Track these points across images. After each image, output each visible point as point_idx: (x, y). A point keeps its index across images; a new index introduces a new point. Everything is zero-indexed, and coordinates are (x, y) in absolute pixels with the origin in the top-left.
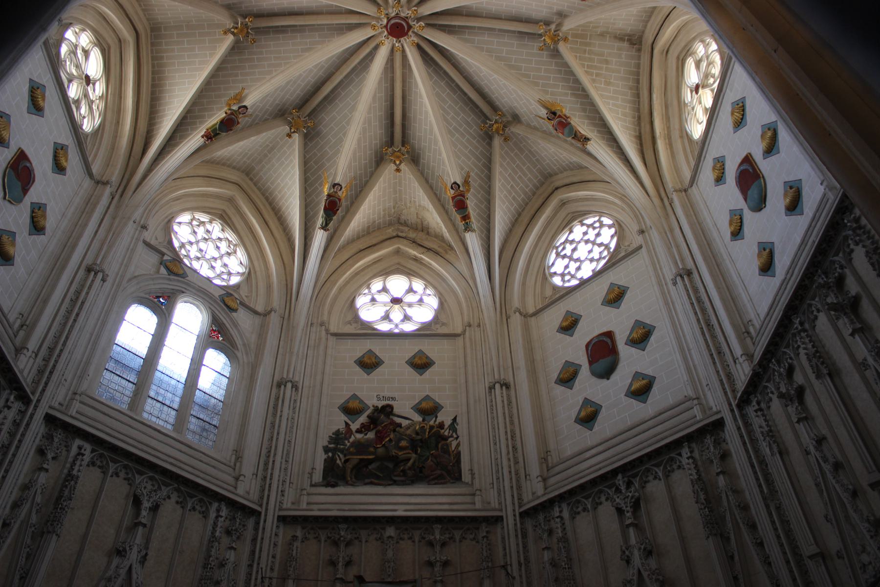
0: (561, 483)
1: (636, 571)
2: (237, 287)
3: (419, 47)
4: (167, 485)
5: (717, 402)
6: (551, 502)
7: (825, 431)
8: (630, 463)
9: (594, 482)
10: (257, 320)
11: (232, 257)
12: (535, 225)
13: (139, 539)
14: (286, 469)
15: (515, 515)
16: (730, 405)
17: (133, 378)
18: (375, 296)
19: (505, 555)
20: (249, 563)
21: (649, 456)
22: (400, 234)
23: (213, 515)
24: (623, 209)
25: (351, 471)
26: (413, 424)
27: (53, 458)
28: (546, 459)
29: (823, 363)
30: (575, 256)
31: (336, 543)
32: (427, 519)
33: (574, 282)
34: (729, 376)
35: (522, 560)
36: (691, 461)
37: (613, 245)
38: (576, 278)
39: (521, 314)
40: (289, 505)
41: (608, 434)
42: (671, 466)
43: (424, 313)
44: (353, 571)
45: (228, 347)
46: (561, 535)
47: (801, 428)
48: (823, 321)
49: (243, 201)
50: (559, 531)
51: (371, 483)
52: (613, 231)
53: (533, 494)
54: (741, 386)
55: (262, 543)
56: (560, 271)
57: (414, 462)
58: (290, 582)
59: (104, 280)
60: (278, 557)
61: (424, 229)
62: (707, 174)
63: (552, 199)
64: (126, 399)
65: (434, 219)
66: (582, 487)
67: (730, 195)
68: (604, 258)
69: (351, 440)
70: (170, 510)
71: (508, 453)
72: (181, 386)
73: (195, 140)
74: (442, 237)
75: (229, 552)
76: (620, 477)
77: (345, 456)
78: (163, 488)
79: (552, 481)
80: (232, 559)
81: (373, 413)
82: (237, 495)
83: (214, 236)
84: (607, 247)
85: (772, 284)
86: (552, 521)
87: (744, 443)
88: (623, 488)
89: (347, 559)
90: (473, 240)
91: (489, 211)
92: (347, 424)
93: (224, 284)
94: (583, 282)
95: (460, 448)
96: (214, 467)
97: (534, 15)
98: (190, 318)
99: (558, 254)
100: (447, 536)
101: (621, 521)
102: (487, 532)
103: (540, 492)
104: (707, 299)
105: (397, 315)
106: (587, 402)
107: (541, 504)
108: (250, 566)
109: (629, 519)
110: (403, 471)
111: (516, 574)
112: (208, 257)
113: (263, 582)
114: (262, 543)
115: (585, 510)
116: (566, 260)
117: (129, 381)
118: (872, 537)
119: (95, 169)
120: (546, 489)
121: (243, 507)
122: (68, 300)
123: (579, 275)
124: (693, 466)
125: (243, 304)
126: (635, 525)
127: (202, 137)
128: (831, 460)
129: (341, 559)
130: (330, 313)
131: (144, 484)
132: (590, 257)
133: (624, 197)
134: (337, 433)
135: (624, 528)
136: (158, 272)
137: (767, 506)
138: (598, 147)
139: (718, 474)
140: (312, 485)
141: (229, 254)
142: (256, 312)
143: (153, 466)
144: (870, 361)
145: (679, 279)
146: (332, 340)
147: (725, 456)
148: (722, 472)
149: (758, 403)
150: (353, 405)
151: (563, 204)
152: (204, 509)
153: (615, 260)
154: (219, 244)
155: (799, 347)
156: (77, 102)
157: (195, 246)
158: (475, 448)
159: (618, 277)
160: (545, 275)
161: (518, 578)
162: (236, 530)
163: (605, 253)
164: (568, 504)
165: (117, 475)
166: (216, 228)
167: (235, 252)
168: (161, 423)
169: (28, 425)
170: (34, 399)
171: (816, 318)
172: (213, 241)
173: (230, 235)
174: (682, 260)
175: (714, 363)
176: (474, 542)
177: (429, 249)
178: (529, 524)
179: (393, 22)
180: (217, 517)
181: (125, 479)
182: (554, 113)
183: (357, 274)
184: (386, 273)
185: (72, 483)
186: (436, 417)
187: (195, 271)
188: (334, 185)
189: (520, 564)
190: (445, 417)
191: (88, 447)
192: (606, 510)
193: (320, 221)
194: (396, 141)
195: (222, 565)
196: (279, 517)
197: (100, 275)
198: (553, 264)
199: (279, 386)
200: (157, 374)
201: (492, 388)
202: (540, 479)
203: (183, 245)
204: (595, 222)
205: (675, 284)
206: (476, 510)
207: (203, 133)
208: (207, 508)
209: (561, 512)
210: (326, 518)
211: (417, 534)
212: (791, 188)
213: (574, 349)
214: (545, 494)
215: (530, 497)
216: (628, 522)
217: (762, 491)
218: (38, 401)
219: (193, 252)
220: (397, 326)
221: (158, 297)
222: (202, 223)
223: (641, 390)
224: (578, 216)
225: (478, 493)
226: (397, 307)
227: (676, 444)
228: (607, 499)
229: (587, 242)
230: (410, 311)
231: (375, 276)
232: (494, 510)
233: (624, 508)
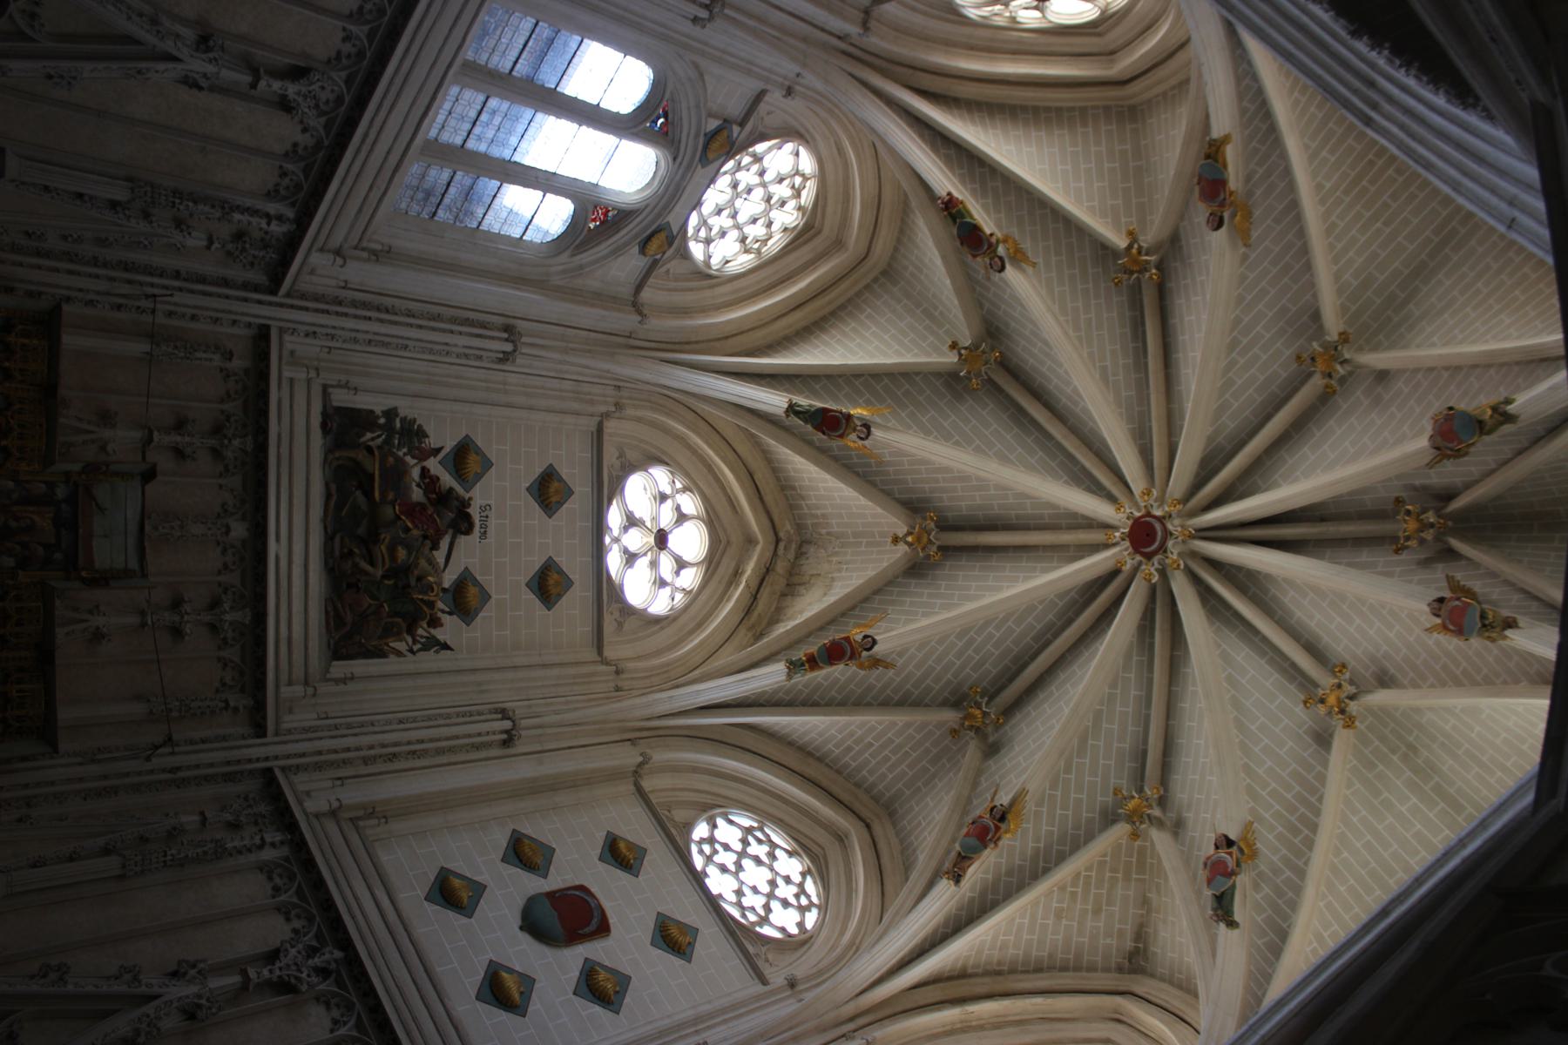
1: (156, 990)
2: (685, 255)
3: (1114, 573)
4: (327, 127)
6: (291, 826)
8: (365, 973)
9: (328, 905)
10: (626, 291)
11: (737, 246)
12: (800, 789)
13: (229, 75)
14: (355, 341)
15: (267, 759)
17: (522, 69)
18: (669, 502)
19: (192, 742)
21: (376, 1009)
22: (782, 545)
23: (272, 208)
24: (833, 948)
26: (439, 572)
28: (371, 815)
30: (746, 863)
31: (217, 430)
32: (261, 597)
33: (698, 862)
35: (181, 774)
37: (767, 931)
38: (706, 865)
39: (640, 765)
40: (289, 346)
41: (420, 931)
43: (638, 588)
45: (576, 237)
46: (229, 845)
49: (837, 264)
50: (236, 843)
51: (328, 496)
52: (794, 930)
53: (308, 793)
56: (718, 834)
57: (366, 573)
59: (695, 20)
60: (193, 325)
61: (793, 586)
63: (846, 818)
64: (485, 57)
65: (810, 606)
66: (319, 884)
68: (744, 916)
69: (408, 459)
70: (282, 132)
71: (383, 746)
72: (506, 154)
73: (943, 181)
74: (778, 621)
76: (338, 954)
77: (379, 447)
78: (323, 120)
79: (331, 827)
80: (190, 242)
81: (458, 498)
82: (310, 250)
83: (774, 214)
84: (764, 920)
88: (317, 961)
90: (772, 676)
91: (827, 705)
92: (439, 450)
93: (690, 231)
94: (698, 878)
95: (392, 658)
96: (360, 210)
97: (1177, 778)
98: (629, 170)
99: (749, 830)
100: (230, 634)
102: (236, 710)
103: (310, 805)
105: (636, 540)
106: (479, 889)
107: (288, 808)
108: (177, 275)
110: (351, 553)
112: (738, 203)
113: (147, 296)
115: (276, 889)
116: (738, 847)
117: (516, 63)
120: (317, 816)
121: (285, 262)
125: (654, 264)
126: (245, 986)
127: (949, 194)
129: (187, 439)
130: (639, 420)
132: (746, 890)
133: (855, 948)
134: (421, 434)
136: (710, 115)
138: (943, 899)
140: (325, 388)
141: (743, 240)
142: (639, 288)
143: (361, 103)
150: (473, 462)
151: (841, 839)
152: (283, 192)
153: (740, 935)
154: (760, 222)
157: (757, 180)
158: (394, 684)
159: (710, 942)
160: (710, 808)
162: (244, 250)
163: (752, 918)
164: (287, 859)
165: (347, 39)
166: (787, 217)
167: (747, 251)
168: (441, 118)
172: (766, 212)
173: (776, 243)
177: (755, 597)
179: (1158, 527)
180: (268, 217)
182: (1002, 818)
183: (710, 468)
184: (712, 521)
186: (450, 613)
187: (713, 181)
188: (867, 426)
190: (450, 628)
192: (275, 930)
193: (803, 401)
194: (948, 536)
195: (179, 224)
196: (268, 327)
197: (704, 14)
198: (731, 822)
199: (507, 329)
200: (529, 113)
201: (504, 714)
202: (335, 805)
203: (758, 159)
204: (808, 897)
206: (277, 686)
207: (956, 194)
209: (273, 845)
210: (264, 413)
213: (576, 864)
214: (306, 814)
215: (301, 788)
216: (252, 973)
219: (747, 178)
220: (616, 540)
221: (666, 116)
222: (797, 193)
223: (501, 991)
224: (819, 867)
225: (310, 691)
226: (652, 540)
228: (295, 931)
229: (773, 883)
230: (643, 563)
231: (706, 500)
232: (277, 723)
233: (278, 964)
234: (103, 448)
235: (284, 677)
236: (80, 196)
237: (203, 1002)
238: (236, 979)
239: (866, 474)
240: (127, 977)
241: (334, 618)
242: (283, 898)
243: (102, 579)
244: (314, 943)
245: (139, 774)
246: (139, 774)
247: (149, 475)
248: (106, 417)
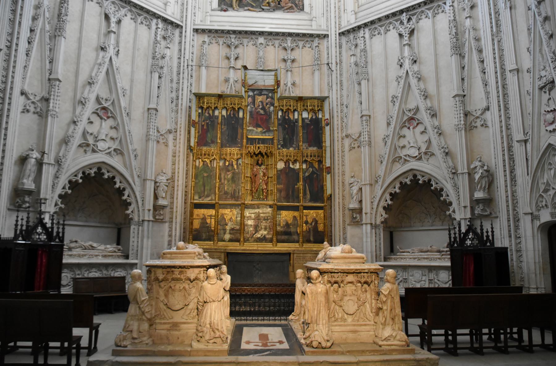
1: (405, 72)
4: (124, 7)
6: (359, 27)
8: (412, 6)
9: (387, 17)
19: (328, 58)
20: (179, 56)
23: (154, 27)
31: (229, 46)
32: (284, 34)
35: (338, 61)
36: (451, 8)
40: (199, 22)
42: (438, 10)
44: (239, 64)
46: (363, 47)
50: (362, 45)
51: (249, 10)
53: (348, 22)
55: (185, 45)
58: (204, 68)
60: (195, 53)
66: (380, 19)
75: (166, 49)
76: (404, 14)
78: (121, 9)
86: (358, 39)
88: (405, 22)
89: (236, 56)
100: (295, 44)
101: (401, 42)
102: (319, 44)
103: (353, 21)
107: (353, 28)
108: (179, 58)
109: (406, 40)
111: (334, 68)
114: (185, 45)
120: (356, 19)
121: (172, 23)
124: (452, 11)
128: (544, 15)
129: (232, 56)
135: (402, 46)
137: (493, 40)
139: (466, 18)
140: (212, 10)
148: (470, 17)
152: (148, 23)
161: (335, 71)
162: (169, 37)
164: (370, 30)
176: (310, 49)
178: (344, 39)
180: (157, 29)
181: (97, 3)
185: (66, 5)
192: (393, 35)
195: (163, 58)
196: (194, 29)
202: (353, 12)
208: (150, 23)
209: (364, 34)
210: (223, 31)
211: (277, 43)
215: (346, 24)
217: (492, 31)
225: (314, 19)
228: (394, 28)
233: (404, 34)
234: (236, 81)
235: (310, 28)
236: (158, 87)
240: (399, 79)
242: (382, 32)
243: (278, 83)
244: (399, 22)
245: (337, 74)
246: (337, 74)
247: (245, 68)
248: (227, 80)
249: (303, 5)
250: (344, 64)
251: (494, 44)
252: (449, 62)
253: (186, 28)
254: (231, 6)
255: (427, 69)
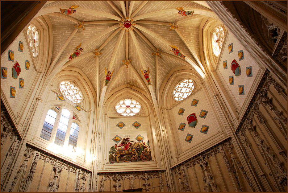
0: (182, 159)
1: (208, 184)
3: (133, 30)
5: (229, 133)
6: (180, 165)
7: (263, 138)
16: (233, 133)
21: (209, 149)
23: (78, 173)
25: (118, 158)
26: (136, 143)
27: (29, 157)
28: (177, 152)
29: (262, 119)
30: (182, 91)
33: (182, 99)
34: (232, 125)
36: (222, 150)
37: (193, 88)
41: (196, 144)
42: (216, 152)
43: (137, 110)
47: (256, 138)
48: (261, 106)
51: (124, 162)
52: (193, 84)
54: (236, 126)
60: (98, 185)
62: (221, 66)
63: (173, 75)
67: (229, 72)
68: (191, 92)
69: (117, 149)
70: (65, 171)
79: (180, 158)
80: (84, 187)
84: (191, 88)
85: (244, 97)
87: (238, 144)
88: (202, 159)
89: (119, 185)
90: (151, 88)
92: (115, 144)
93: (76, 103)
94: (185, 99)
97: (168, 20)
98: (66, 113)
99: (176, 91)
104: (224, 103)
105: (128, 111)
106: (188, 135)
107: (177, 165)
111: (171, 186)
115: (190, 166)
116: (179, 93)
118: (280, 168)
119: (37, 68)
122: (31, 108)
123: (183, 97)
128: (266, 147)
131: (57, 164)
132: (186, 91)
134: (113, 147)
135: (204, 171)
137: (247, 162)
138: (188, 59)
139: (231, 153)
140: (107, 163)
144: (277, 117)
145: (215, 97)
146: (109, 118)
147: (232, 148)
148: (232, 153)
149: (242, 132)
151: (177, 76)
153: (194, 92)
155: (254, 114)
156: (32, 48)
157: (66, 91)
159: (196, 97)
160: (173, 98)
163: (191, 90)
164: (185, 165)
166: (73, 86)
169: (21, 147)
170: (23, 139)
171: (259, 106)
172: (72, 90)
173: (76, 88)
174: (216, 91)
175: (228, 121)
176: (157, 178)
180: (79, 174)
188: (109, 72)
189: (172, 184)
191: (39, 153)
192: (197, 166)
193: (105, 83)
194: (128, 59)
197: (40, 100)
205: (214, 98)
210: (112, 173)
211: (140, 177)
212: (248, 69)
213: (184, 119)
217: (245, 158)
218: (24, 139)
219: (66, 93)
220: (128, 114)
223: (205, 130)
224: (181, 80)
225: (157, 163)
227: (218, 145)
228: (197, 163)
229: (185, 87)
230: (132, 110)
231: (121, 99)
237: (209, 176)
238: (206, 172)
239: (116, 72)
241: (145, 160)
249: (151, 157)
250: (176, 184)
251: (248, 164)
252: (228, 175)
253: (93, 173)
254: (116, 161)
255: (219, 180)
